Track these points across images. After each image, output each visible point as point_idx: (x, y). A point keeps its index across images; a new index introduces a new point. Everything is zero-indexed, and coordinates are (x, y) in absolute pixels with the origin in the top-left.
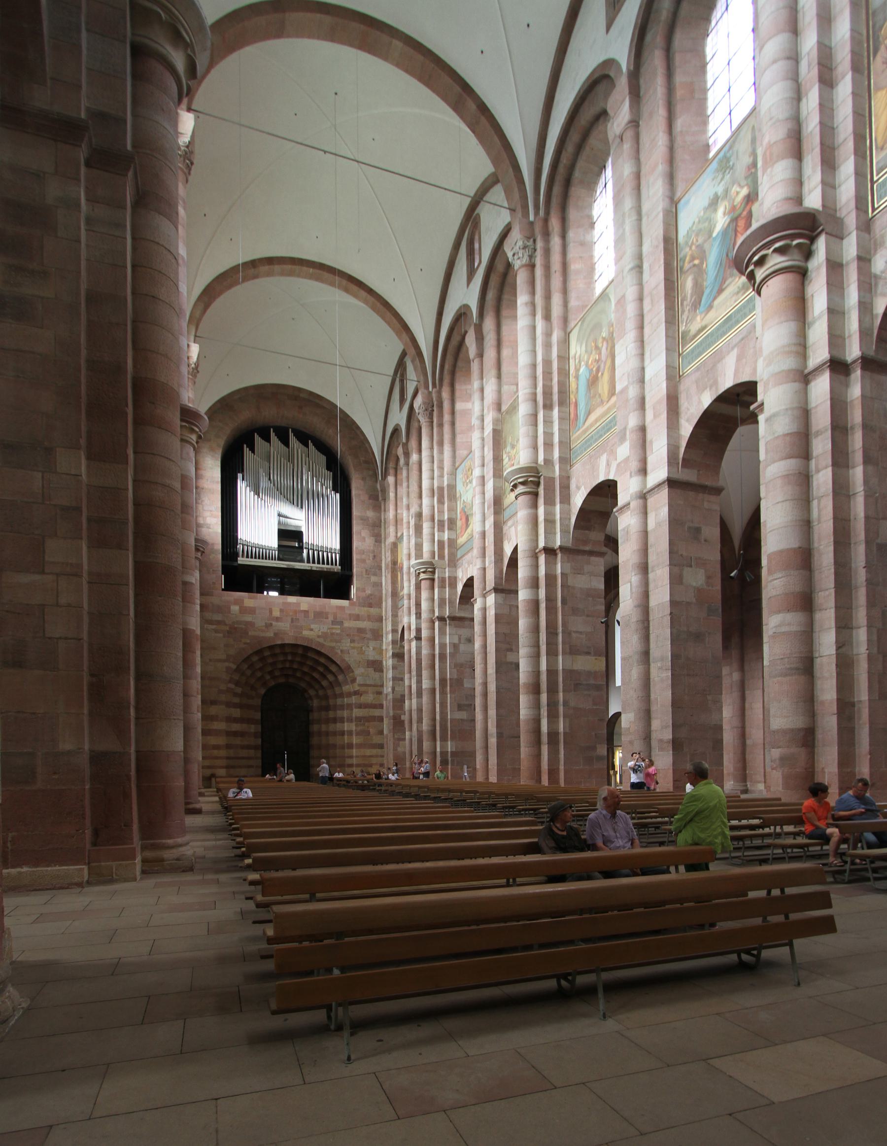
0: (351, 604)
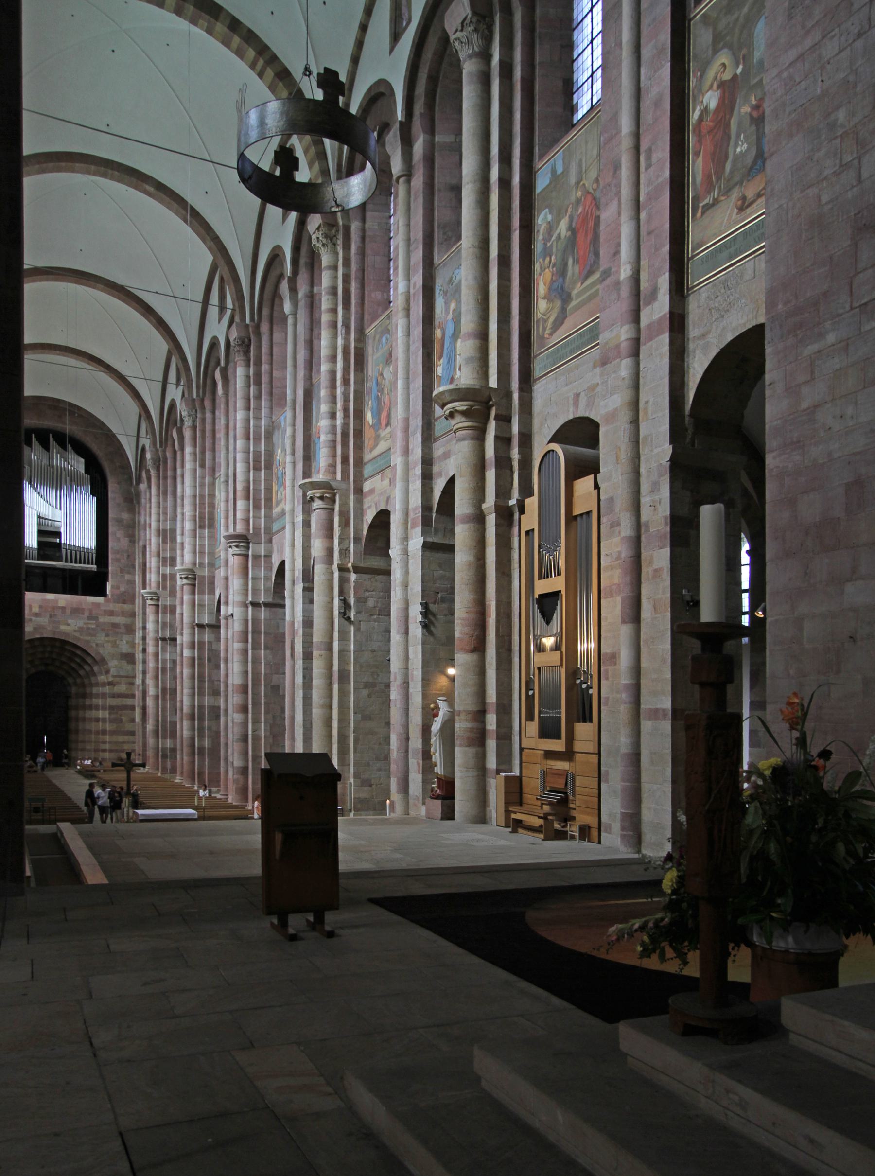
0: (105, 601)
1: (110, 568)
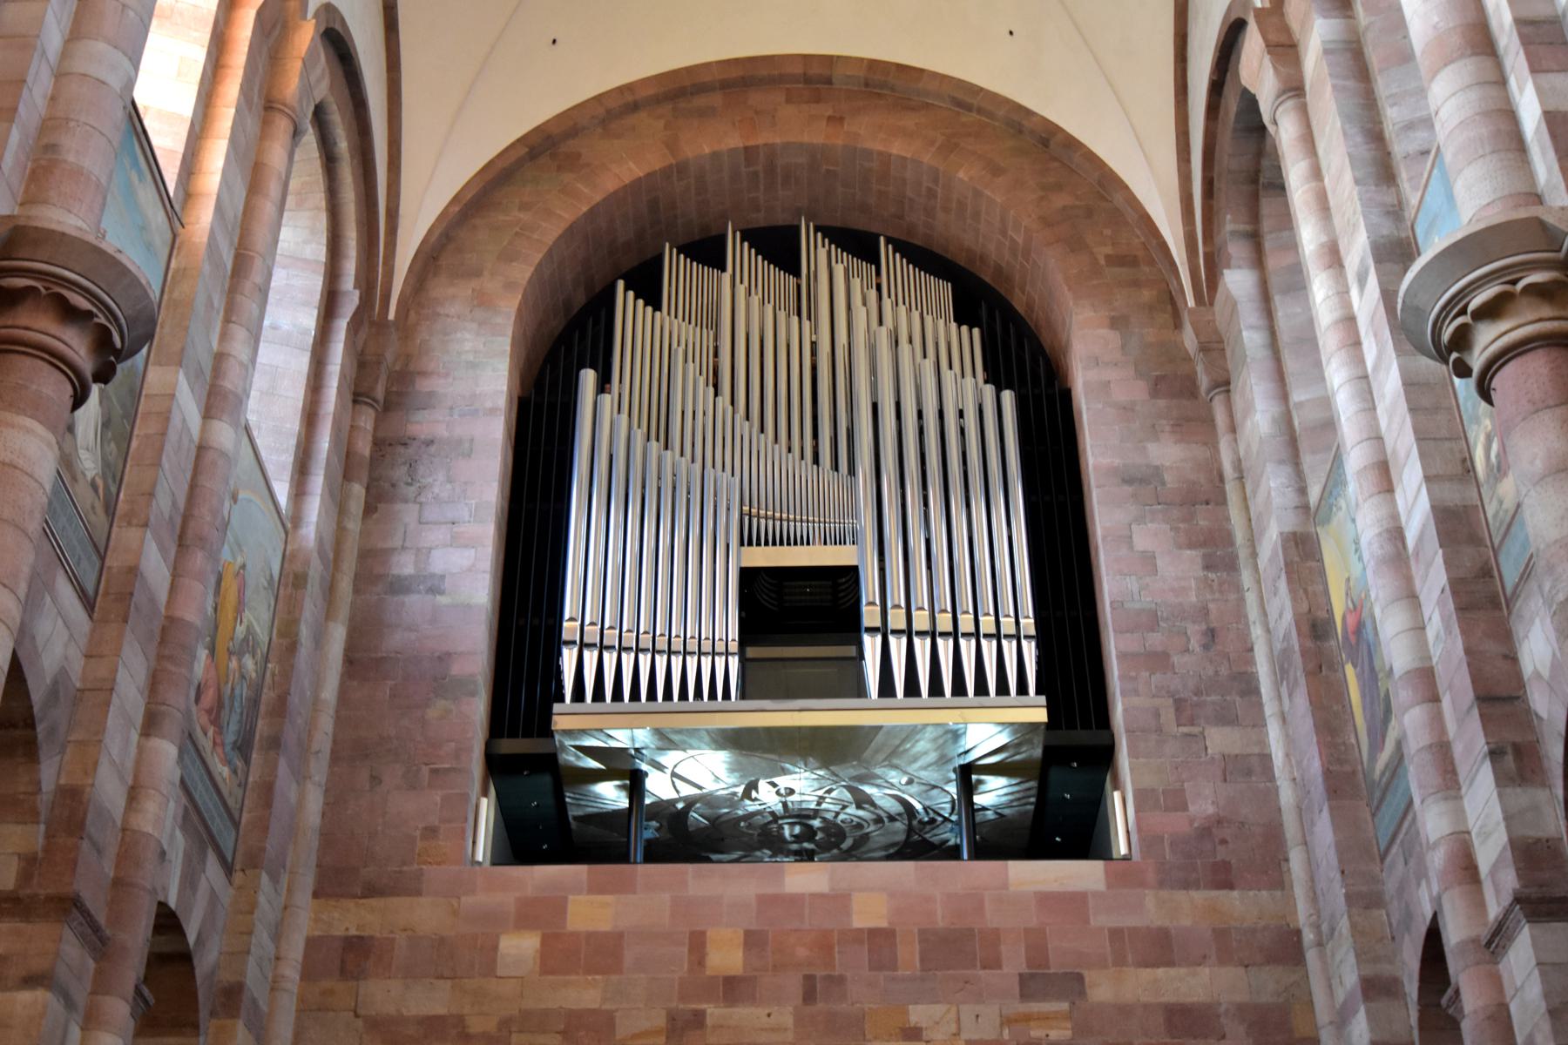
0: (1113, 880)
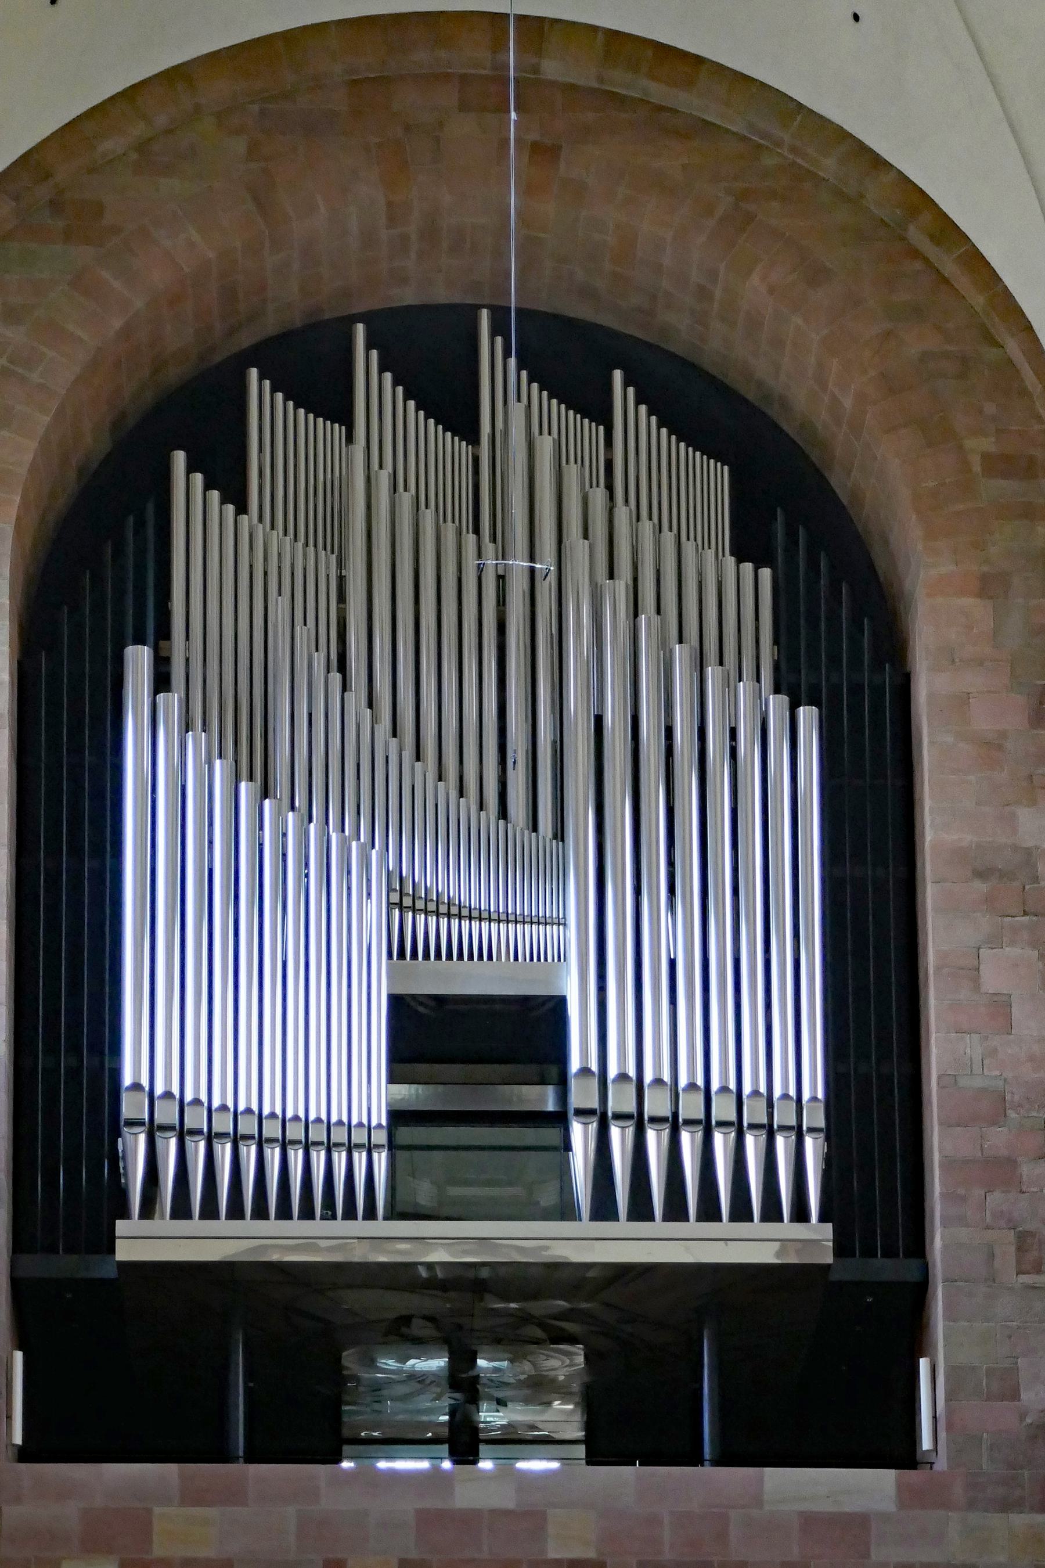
0: (907, 1498)
1: (938, 1242)
